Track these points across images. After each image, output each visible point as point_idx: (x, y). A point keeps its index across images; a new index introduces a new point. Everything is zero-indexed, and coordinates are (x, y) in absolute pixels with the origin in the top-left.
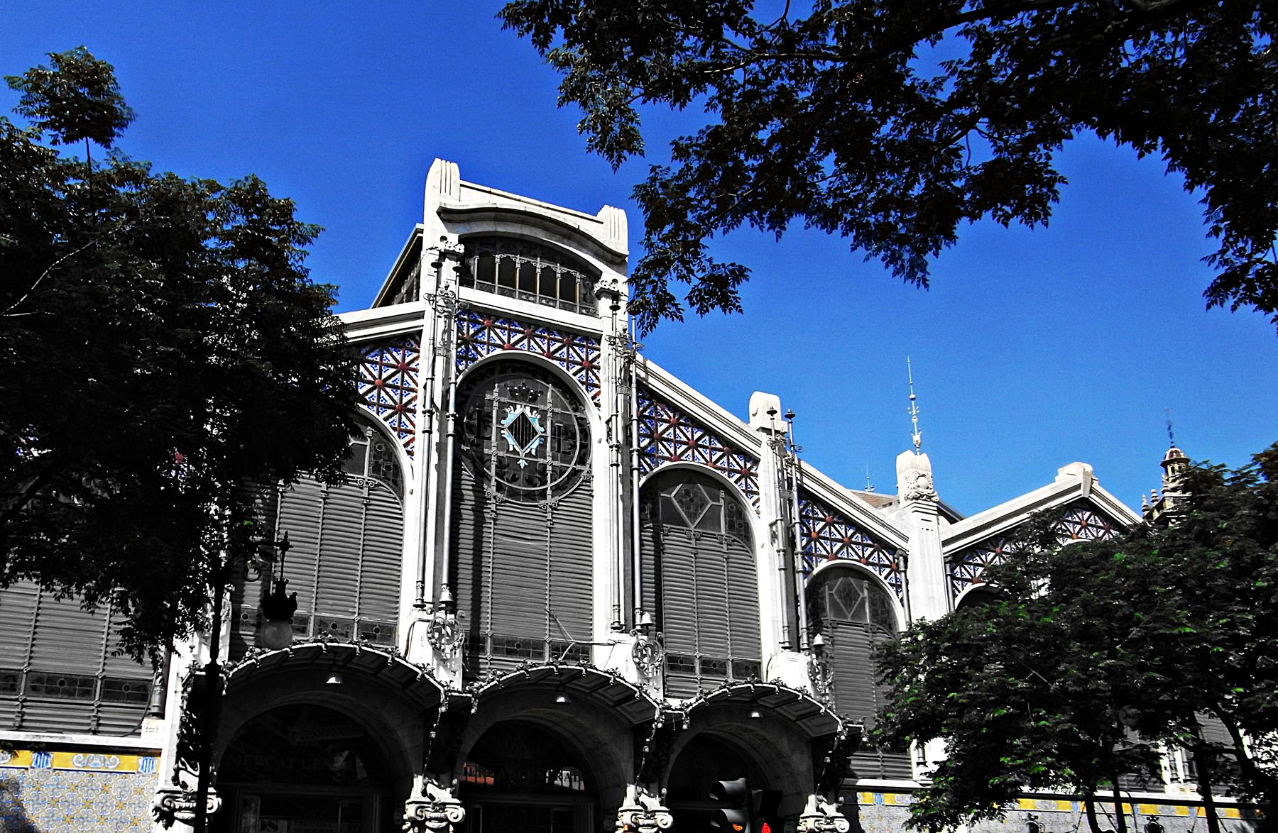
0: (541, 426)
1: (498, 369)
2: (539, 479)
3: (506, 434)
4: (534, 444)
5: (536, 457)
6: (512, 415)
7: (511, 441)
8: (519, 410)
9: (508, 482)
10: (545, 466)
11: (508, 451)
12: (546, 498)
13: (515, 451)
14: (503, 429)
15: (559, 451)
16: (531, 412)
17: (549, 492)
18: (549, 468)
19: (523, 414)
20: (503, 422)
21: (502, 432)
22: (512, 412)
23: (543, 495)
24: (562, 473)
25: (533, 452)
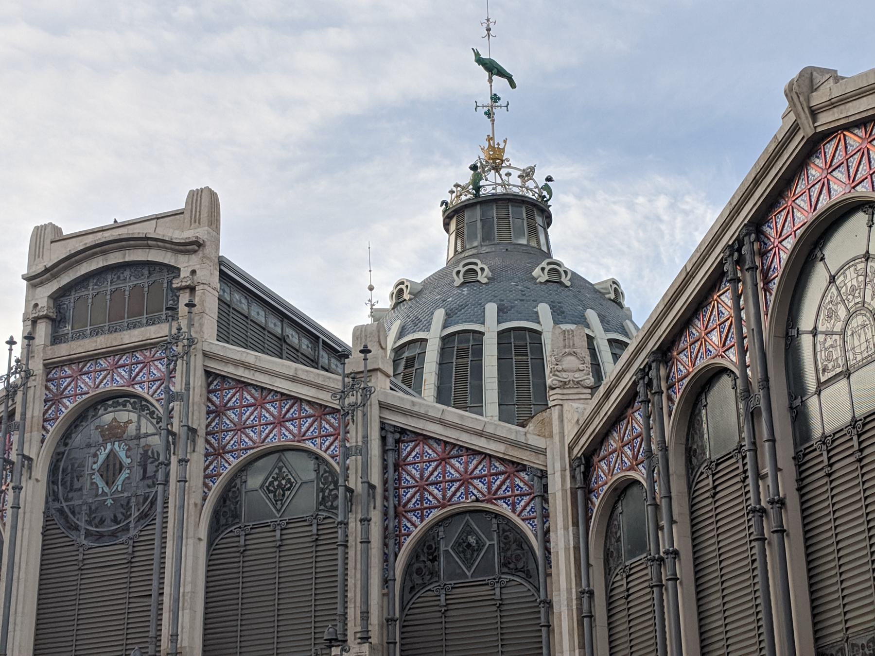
0: (127, 457)
2: (123, 514)
3: (97, 479)
5: (122, 492)
6: (102, 457)
7: (101, 484)
9: (97, 527)
10: (128, 503)
12: (128, 530)
13: (104, 494)
14: (93, 474)
15: (144, 477)
16: (119, 447)
17: (132, 525)
18: (133, 499)
19: (112, 450)
20: (95, 466)
21: (93, 477)
22: (103, 453)
23: (126, 529)
24: (146, 499)
25: (119, 489)
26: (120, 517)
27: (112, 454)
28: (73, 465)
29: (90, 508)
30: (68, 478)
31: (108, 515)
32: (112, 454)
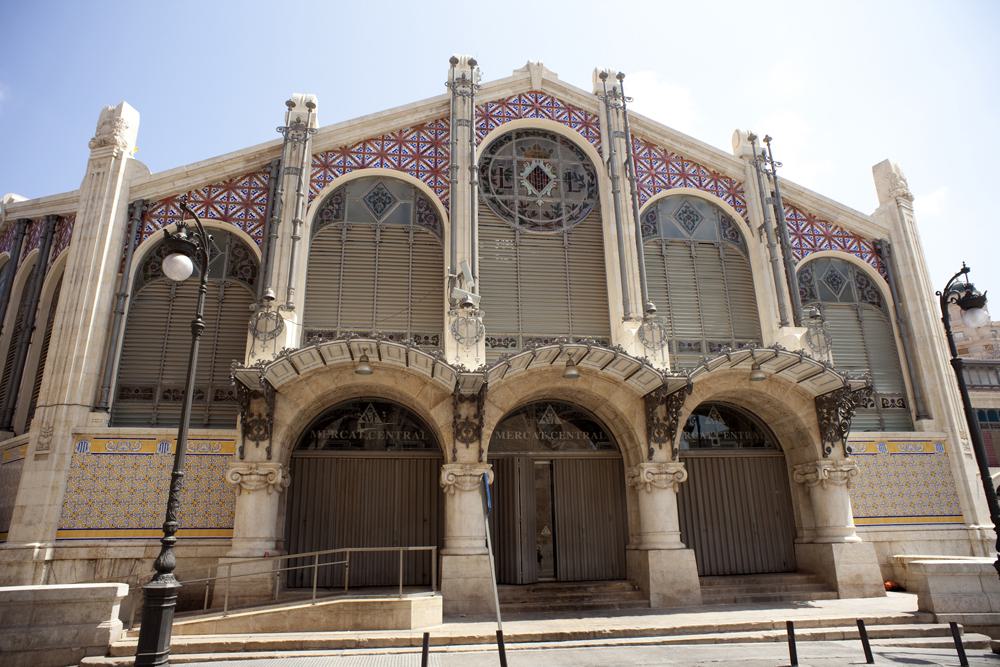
1: (514, 136)
3: (526, 183)
4: (548, 189)
6: (528, 170)
7: (530, 188)
8: (534, 165)
10: (559, 204)
11: (527, 195)
15: (570, 190)
17: (564, 222)
18: (563, 204)
24: (574, 208)
25: (549, 194)
26: (551, 214)
27: (537, 169)
28: (501, 169)
29: (521, 203)
30: (498, 177)
31: (541, 211)
32: (538, 170)
